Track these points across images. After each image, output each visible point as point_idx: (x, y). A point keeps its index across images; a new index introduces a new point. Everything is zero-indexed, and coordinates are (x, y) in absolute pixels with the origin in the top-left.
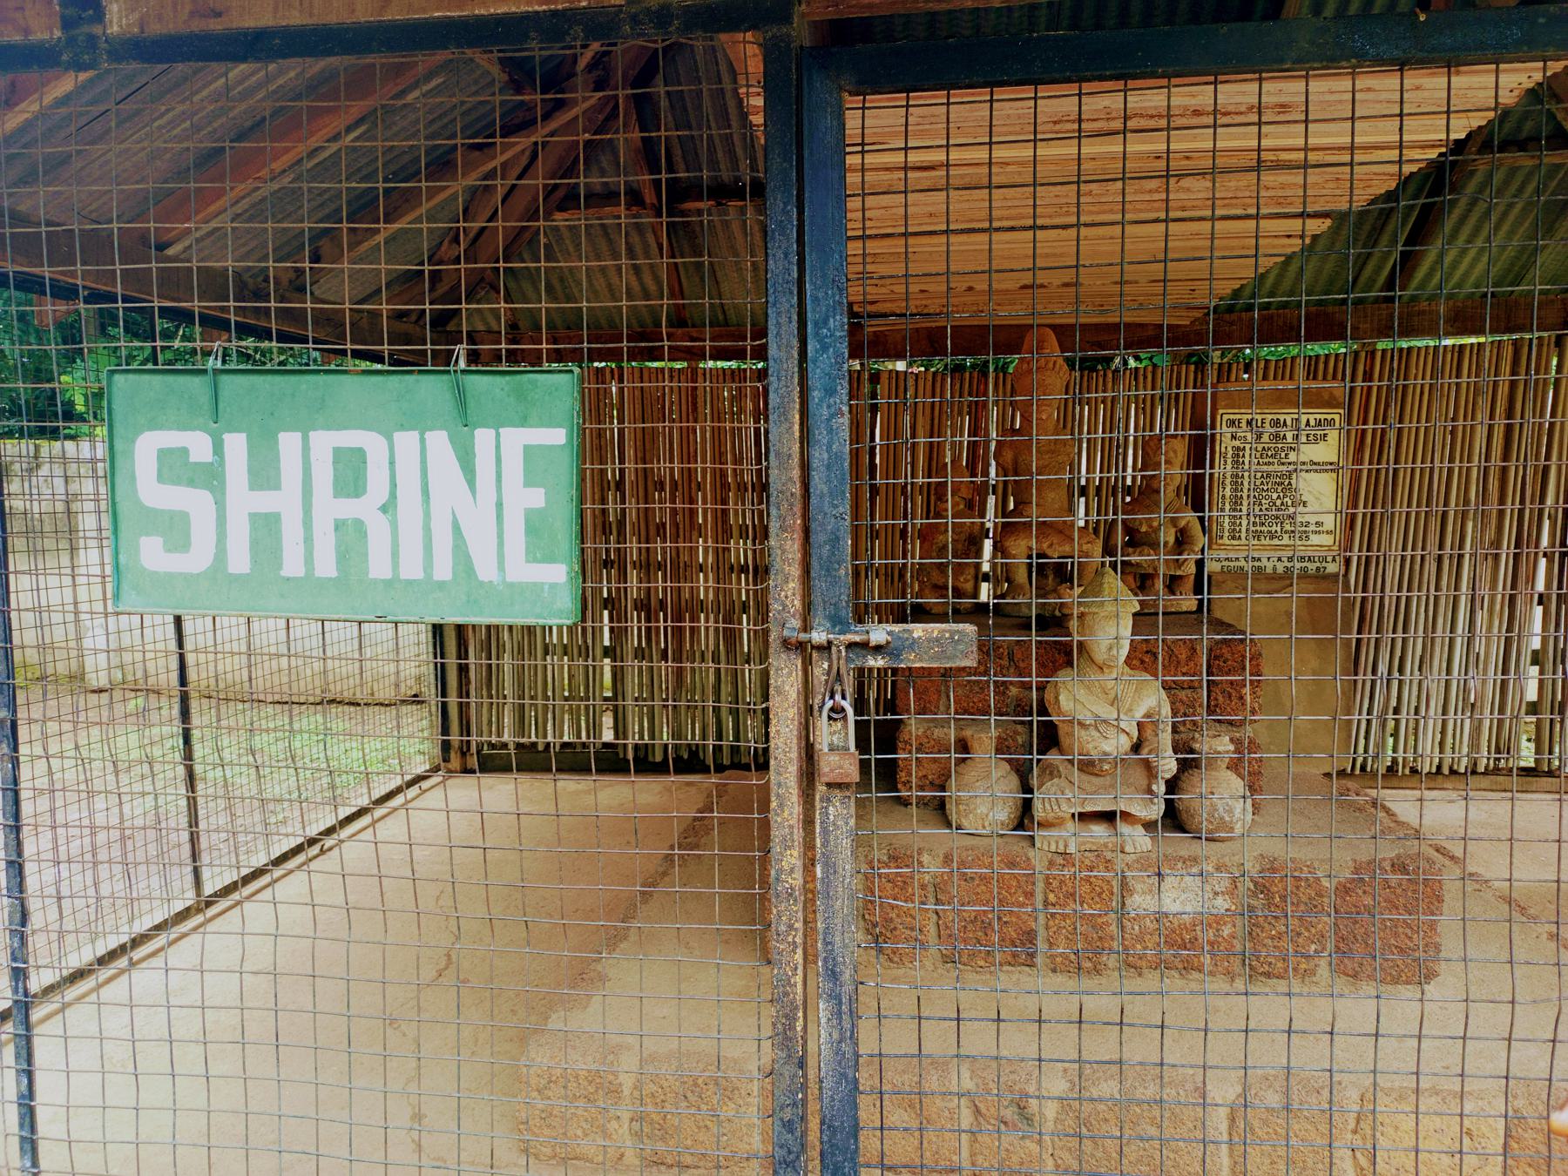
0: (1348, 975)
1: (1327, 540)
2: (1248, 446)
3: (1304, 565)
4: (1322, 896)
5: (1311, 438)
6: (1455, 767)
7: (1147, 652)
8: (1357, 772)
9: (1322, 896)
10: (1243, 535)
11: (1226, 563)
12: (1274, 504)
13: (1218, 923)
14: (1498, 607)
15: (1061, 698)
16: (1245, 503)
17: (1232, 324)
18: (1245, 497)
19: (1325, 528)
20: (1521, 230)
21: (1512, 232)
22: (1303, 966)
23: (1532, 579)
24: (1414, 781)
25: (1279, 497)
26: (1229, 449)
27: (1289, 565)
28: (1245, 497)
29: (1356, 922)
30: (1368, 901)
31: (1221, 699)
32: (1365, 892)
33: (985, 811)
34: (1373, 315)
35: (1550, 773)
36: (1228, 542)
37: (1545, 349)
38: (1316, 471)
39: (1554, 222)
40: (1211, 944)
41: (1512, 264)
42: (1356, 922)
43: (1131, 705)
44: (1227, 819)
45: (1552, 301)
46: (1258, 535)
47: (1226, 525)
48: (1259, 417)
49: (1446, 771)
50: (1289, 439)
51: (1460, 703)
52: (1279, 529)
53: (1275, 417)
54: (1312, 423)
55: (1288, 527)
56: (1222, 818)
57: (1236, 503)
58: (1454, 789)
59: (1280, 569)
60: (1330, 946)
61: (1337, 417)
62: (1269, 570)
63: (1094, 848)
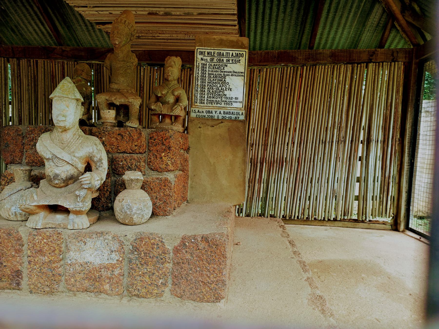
0: (179, 297)
1: (240, 105)
2: (208, 64)
3: (230, 116)
4: (165, 253)
5: (234, 61)
6: (329, 218)
7: (119, 134)
8: (296, 218)
9: (165, 253)
10: (205, 102)
11: (198, 114)
12: (218, 89)
13: (113, 268)
14: (345, 160)
15: (37, 145)
16: (206, 88)
17: (255, 54)
18: (206, 86)
19: (239, 100)
20: (354, 25)
21: (351, 26)
22: (156, 291)
23: (356, 151)
24: (316, 223)
25: (220, 86)
26: (200, 64)
27: (224, 115)
28: (206, 86)
29: (182, 268)
30: (188, 256)
31: (152, 158)
32: (186, 252)
33: (9, 207)
34: (303, 53)
35: (363, 221)
36: (199, 105)
37: (362, 68)
38: (235, 75)
39: (365, 22)
40: (110, 278)
41: (353, 40)
42: (182, 268)
43: (75, 150)
44: (128, 213)
45: (365, 51)
46: (211, 102)
47: (198, 97)
48: (213, 51)
49: (326, 219)
50: (225, 62)
51: (332, 195)
52: (220, 100)
53: (219, 51)
54: (234, 55)
55: (224, 99)
56: (126, 212)
57: (203, 88)
58: (330, 226)
59: (220, 118)
60: (170, 281)
61: (244, 53)
62: (216, 118)
63: (54, 226)
